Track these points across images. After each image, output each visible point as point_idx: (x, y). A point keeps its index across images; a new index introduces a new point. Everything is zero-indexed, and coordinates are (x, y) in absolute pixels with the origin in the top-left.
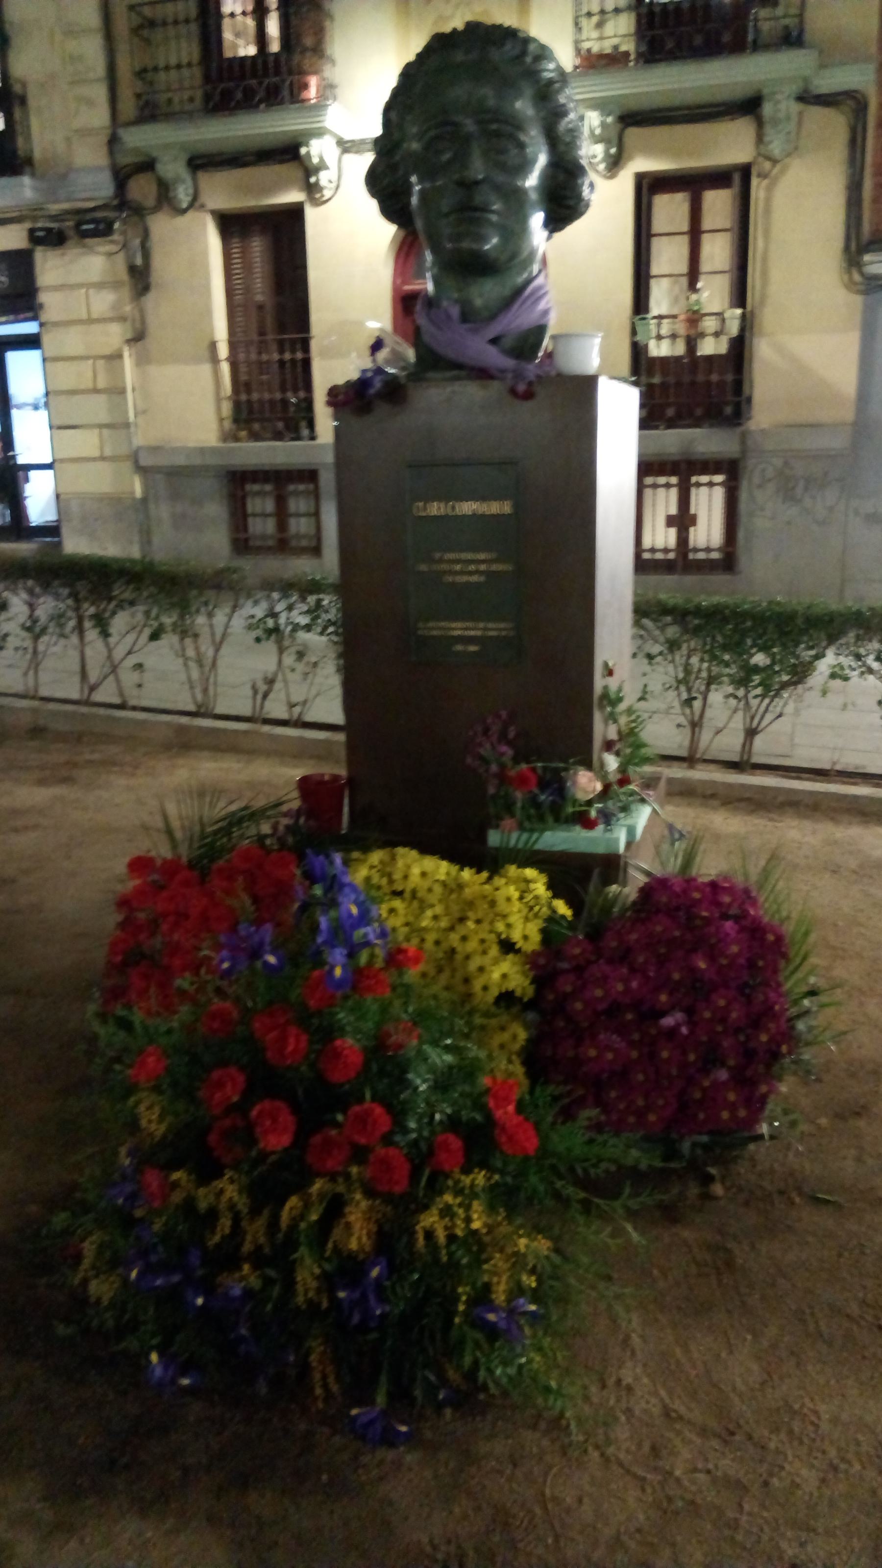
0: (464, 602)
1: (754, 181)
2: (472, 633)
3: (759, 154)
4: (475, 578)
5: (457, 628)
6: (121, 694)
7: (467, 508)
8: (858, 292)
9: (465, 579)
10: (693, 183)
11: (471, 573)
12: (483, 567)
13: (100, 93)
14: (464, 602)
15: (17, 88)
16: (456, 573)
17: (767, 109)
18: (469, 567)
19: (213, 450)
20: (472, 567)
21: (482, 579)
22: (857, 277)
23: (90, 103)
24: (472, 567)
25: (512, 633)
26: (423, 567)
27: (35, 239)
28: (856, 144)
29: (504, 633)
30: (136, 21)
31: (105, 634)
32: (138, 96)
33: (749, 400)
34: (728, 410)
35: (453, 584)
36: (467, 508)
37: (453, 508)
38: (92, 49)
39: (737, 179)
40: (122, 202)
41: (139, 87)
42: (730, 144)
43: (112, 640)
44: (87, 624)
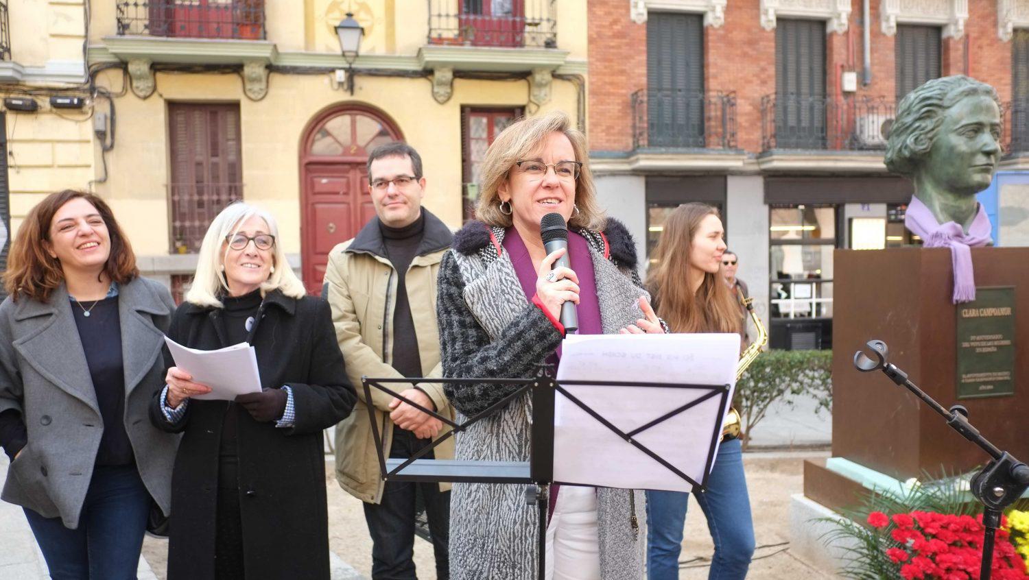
0: (985, 362)
2: (990, 379)
3: (530, 101)
4: (989, 350)
5: (981, 377)
7: (989, 312)
9: (985, 350)
11: (989, 347)
12: (996, 343)
14: (985, 362)
16: (981, 347)
17: (538, 77)
18: (987, 343)
19: (161, 260)
20: (990, 344)
21: (995, 349)
23: (68, 18)
24: (990, 344)
25: (1008, 378)
26: (966, 345)
29: (1006, 378)
35: (981, 353)
36: (989, 312)
37: (982, 312)
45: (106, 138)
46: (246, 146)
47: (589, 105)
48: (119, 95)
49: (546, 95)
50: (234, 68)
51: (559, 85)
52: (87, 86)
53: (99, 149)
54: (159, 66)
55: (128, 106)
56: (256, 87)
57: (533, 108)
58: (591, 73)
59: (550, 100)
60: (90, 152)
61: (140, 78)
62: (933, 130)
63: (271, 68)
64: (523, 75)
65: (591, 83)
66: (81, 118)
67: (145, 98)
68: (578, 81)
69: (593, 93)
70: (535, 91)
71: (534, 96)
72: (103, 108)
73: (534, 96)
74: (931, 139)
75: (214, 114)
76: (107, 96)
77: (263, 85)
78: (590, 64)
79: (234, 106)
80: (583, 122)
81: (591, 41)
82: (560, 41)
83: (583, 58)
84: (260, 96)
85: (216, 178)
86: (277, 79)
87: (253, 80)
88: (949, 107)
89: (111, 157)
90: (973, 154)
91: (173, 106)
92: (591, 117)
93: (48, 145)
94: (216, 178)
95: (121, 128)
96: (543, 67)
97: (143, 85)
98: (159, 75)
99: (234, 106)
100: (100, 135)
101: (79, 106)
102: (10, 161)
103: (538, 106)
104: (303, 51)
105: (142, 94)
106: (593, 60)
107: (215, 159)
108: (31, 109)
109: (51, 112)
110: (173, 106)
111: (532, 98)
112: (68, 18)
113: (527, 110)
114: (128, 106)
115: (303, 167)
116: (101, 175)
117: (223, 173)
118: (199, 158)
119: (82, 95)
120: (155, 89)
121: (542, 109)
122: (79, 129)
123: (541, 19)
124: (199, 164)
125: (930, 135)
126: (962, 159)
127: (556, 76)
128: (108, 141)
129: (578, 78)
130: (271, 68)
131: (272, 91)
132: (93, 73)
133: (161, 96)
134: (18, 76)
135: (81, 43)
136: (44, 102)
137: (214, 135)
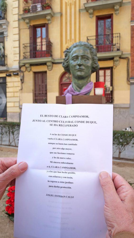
1: (113, 69)
3: (114, 65)
6: (15, 144)
8: (129, 85)
10: (104, 69)
13: (18, 55)
15: (6, 54)
17: (115, 59)
22: (129, 83)
23: (16, 57)
27: (7, 75)
28: (128, 64)
30: (24, 46)
31: (13, 134)
32: (23, 56)
33: (114, 100)
34: (111, 101)
38: (17, 50)
39: (111, 68)
40: (20, 70)
41: (24, 55)
42: (109, 64)
43: (14, 136)
44: (11, 133)
45: (22, 81)
46: (48, 81)
47: (131, 65)
48: (25, 72)
49: (118, 63)
50: (44, 64)
51: (122, 60)
52: (19, 70)
53: (21, 83)
54: (32, 65)
55: (26, 73)
56: (50, 67)
57: (115, 67)
58: (131, 56)
59: (119, 65)
60: (19, 84)
61: (28, 67)
62: (67, 59)
63: (53, 63)
64: (112, 59)
65: (132, 59)
66: (18, 77)
67: (29, 72)
68: (127, 59)
69: (132, 61)
70: (115, 63)
71: (115, 64)
72: (22, 75)
73: (115, 64)
74: (67, 62)
75: (43, 74)
76: (23, 72)
77: (51, 67)
78: (131, 54)
79: (46, 72)
80: (129, 70)
81: (132, 47)
82: (121, 49)
83: (129, 52)
84: (51, 69)
85: (43, 88)
86: (54, 65)
87: (50, 66)
88: (70, 52)
89: (23, 84)
90: (75, 66)
91: (35, 73)
92: (131, 68)
93: (13, 83)
94: (43, 88)
95: (25, 79)
96: (116, 56)
97: (29, 69)
98: (32, 67)
99: (46, 72)
100: (21, 80)
101: (18, 74)
102: (7, 86)
103: (116, 66)
104: (60, 58)
105: (29, 71)
106: (132, 53)
107: (43, 84)
108: (10, 76)
109: (13, 76)
110: (35, 73)
111: (115, 65)
112: (16, 57)
113: (113, 68)
114: (26, 73)
115: (60, 85)
116: (21, 88)
117: (44, 87)
118: (40, 84)
119: (18, 72)
120: (31, 70)
121: (118, 67)
122: (17, 79)
123: (115, 43)
124: (40, 85)
125: (67, 61)
126: (72, 68)
127: (120, 58)
128: (23, 81)
129: (128, 58)
130: (53, 63)
131: (53, 68)
132: (20, 67)
133: (32, 71)
134: (8, 69)
135: (18, 62)
136: (12, 74)
137: (43, 79)
